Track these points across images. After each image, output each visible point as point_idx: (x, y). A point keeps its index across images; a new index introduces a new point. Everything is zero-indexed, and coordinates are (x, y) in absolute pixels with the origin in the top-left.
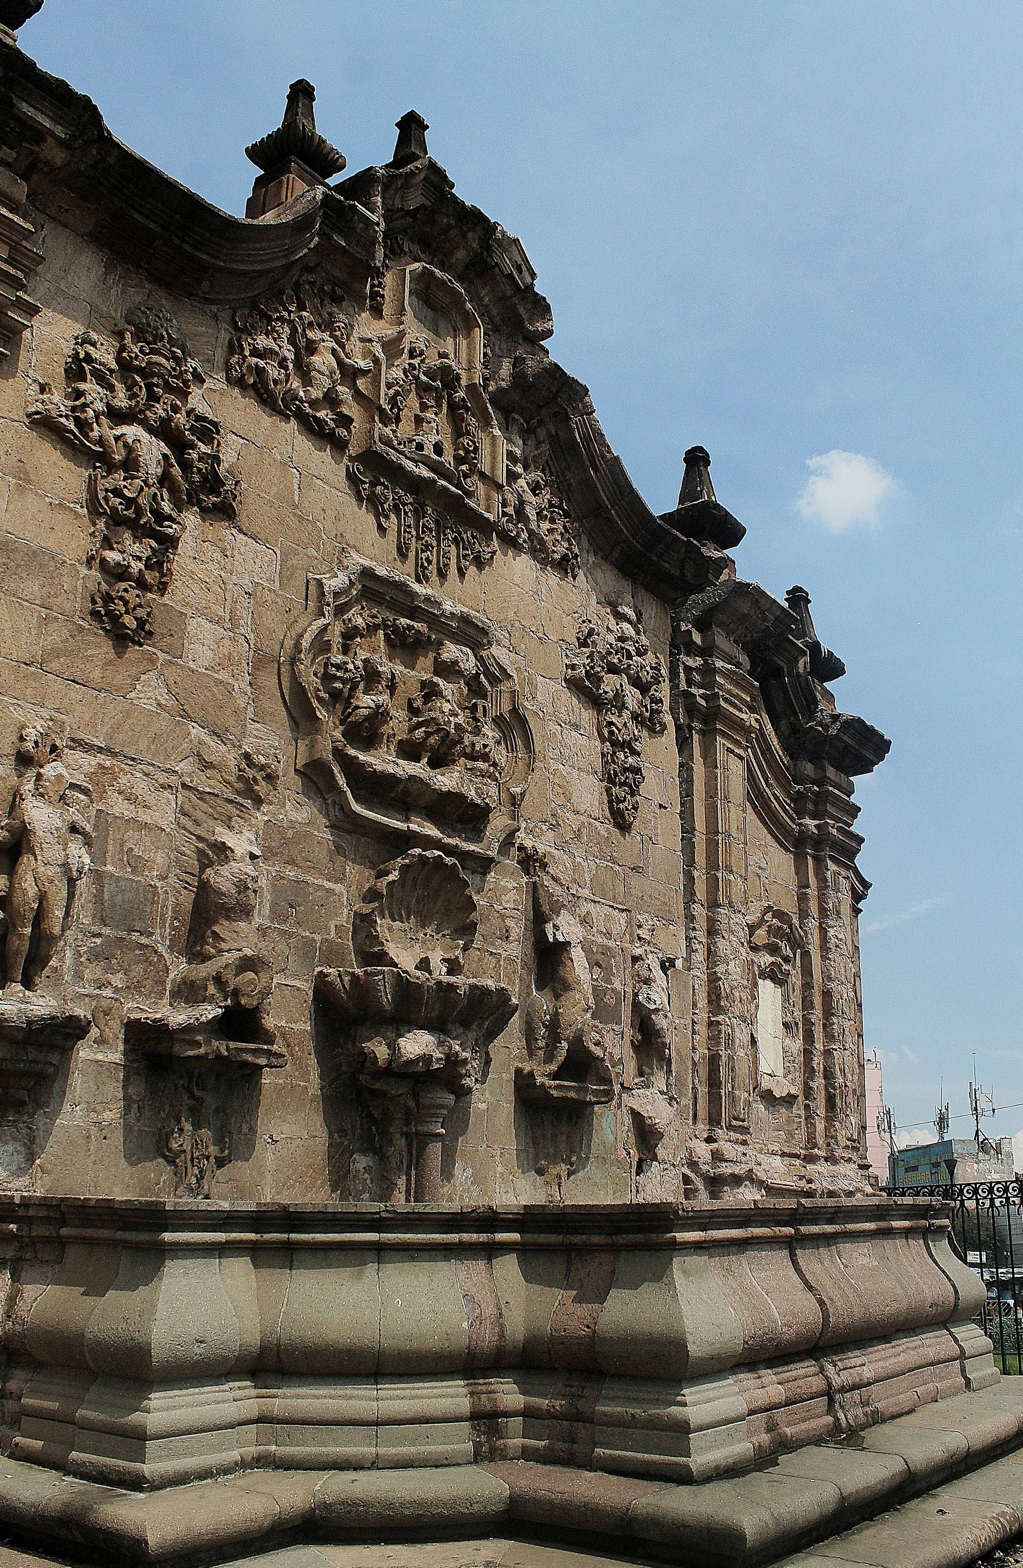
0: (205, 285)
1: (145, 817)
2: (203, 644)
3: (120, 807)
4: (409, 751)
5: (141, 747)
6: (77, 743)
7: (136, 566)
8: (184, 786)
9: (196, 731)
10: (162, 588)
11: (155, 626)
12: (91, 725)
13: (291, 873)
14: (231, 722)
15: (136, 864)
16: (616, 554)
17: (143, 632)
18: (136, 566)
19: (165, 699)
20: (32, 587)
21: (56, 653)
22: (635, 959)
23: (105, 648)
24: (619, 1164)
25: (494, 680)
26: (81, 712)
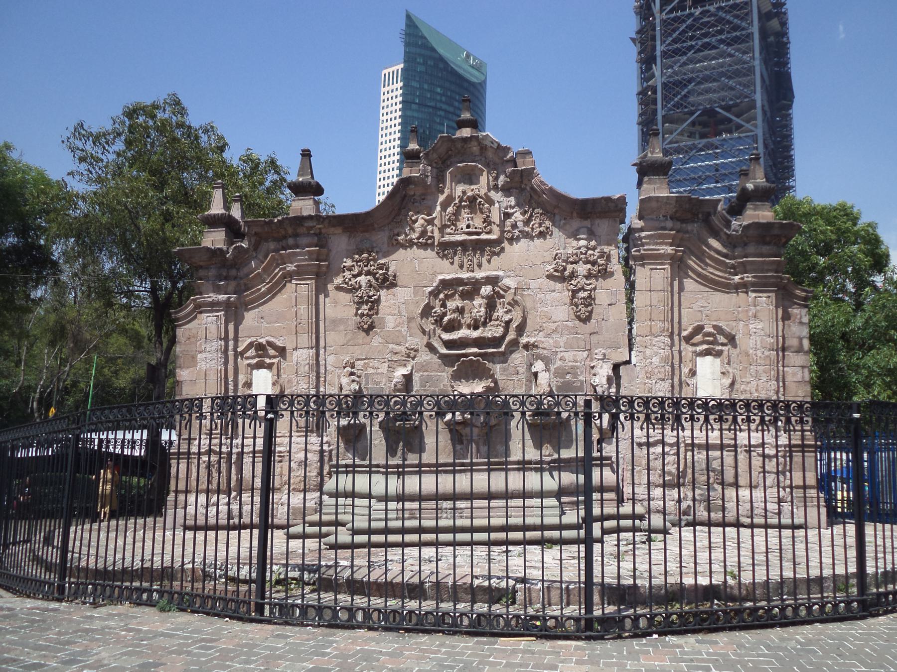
0: (376, 226)
1: (379, 371)
2: (390, 323)
3: (371, 371)
4: (469, 327)
5: (376, 355)
6: (358, 359)
7: (365, 312)
9: (391, 346)
10: (377, 313)
11: (376, 324)
12: (361, 354)
13: (426, 374)
14: (402, 339)
15: (377, 383)
16: (575, 214)
17: (371, 327)
18: (365, 312)
19: (380, 340)
20: (342, 328)
21: (349, 340)
22: (593, 367)
23: (364, 334)
25: (506, 291)
26: (358, 352)
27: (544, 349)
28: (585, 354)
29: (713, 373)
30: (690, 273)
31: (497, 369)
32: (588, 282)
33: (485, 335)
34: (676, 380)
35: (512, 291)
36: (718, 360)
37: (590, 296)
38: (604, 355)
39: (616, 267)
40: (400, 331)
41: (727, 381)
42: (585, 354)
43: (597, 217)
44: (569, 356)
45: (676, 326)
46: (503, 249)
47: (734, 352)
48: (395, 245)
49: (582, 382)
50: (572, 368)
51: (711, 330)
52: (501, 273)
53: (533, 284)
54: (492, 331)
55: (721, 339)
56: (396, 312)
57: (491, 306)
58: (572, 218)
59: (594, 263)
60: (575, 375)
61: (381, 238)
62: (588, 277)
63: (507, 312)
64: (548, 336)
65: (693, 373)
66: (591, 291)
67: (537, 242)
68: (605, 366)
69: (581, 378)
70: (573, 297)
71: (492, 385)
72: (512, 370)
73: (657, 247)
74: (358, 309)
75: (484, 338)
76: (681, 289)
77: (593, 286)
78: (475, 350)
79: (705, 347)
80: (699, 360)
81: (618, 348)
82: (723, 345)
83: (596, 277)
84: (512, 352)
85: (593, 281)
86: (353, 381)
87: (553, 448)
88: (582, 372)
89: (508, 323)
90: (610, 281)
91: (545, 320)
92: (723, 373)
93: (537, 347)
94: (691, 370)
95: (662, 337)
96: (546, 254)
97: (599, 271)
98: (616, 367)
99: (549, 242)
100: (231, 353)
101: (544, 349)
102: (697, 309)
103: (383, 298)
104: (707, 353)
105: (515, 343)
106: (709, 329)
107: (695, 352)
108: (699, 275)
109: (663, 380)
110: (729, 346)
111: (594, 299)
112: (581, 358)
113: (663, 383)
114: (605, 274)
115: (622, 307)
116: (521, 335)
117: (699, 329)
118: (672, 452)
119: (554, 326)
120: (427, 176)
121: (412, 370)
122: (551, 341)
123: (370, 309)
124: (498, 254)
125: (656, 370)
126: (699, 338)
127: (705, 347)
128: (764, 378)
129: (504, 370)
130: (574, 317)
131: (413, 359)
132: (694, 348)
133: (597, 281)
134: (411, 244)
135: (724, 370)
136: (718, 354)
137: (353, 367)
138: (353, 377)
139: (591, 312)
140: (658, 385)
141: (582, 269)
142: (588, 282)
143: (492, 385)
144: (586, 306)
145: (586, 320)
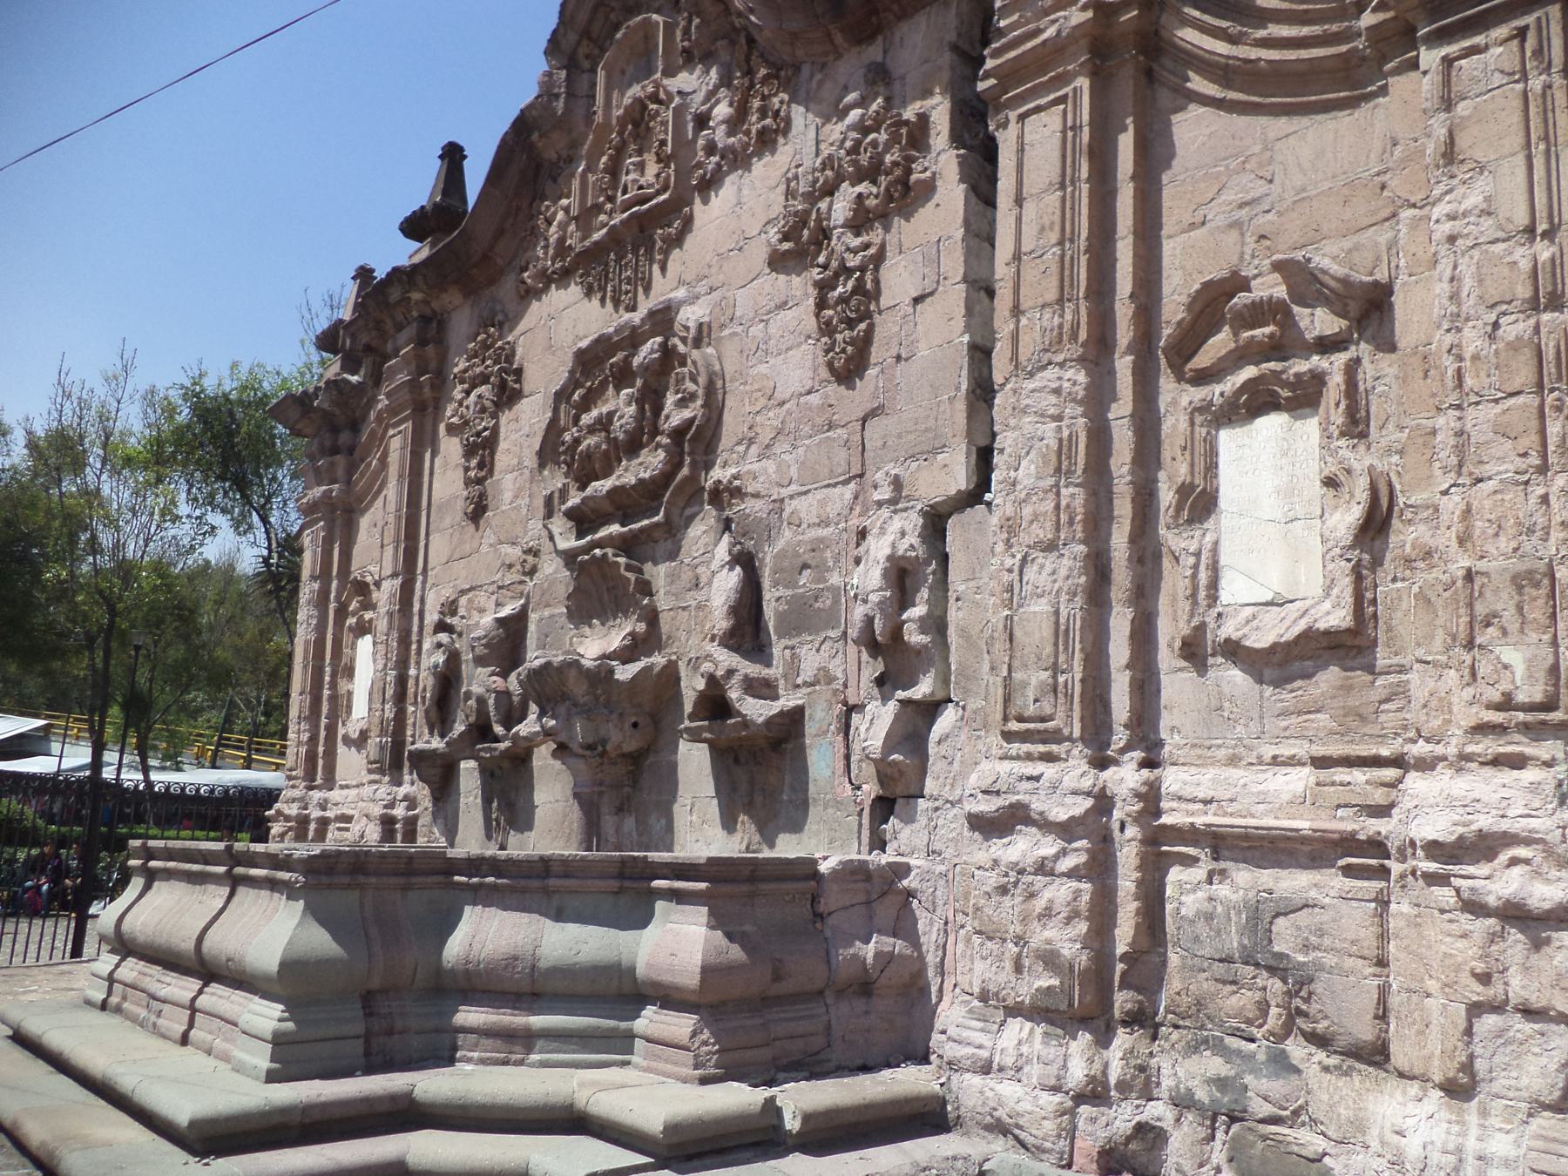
0: (499, 261)
6: (463, 592)
8: (500, 588)
14: (519, 530)
16: (839, 38)
24: (838, 804)
27: (756, 496)
28: (848, 491)
29: (1288, 492)
30: (1198, 83)
31: (658, 573)
32: (856, 242)
33: (624, 480)
34: (1119, 541)
35: (693, 332)
36: (1310, 427)
37: (859, 289)
38: (897, 483)
39: (943, 161)
40: (518, 508)
41: (1346, 518)
42: (848, 491)
43: (899, 19)
44: (805, 507)
45: (1124, 311)
46: (688, 222)
47: (1378, 369)
48: (529, 294)
49: (835, 590)
50: (816, 546)
51: (1281, 292)
52: (681, 293)
53: (743, 302)
54: (651, 462)
55: (1319, 321)
56: (515, 461)
57: (651, 400)
58: (839, 56)
59: (870, 173)
60: (822, 571)
61: (506, 289)
62: (861, 220)
63: (682, 403)
64: (766, 452)
65: (1200, 503)
66: (862, 269)
67: (758, 166)
68: (897, 523)
69: (835, 579)
70: (821, 304)
71: (641, 627)
72: (687, 575)
73: (1032, 26)
74: (467, 469)
75: (623, 487)
76: (1154, 155)
77: (872, 251)
78: (615, 528)
79: (1249, 372)
80: (1228, 439)
81: (935, 451)
82: (1326, 345)
83: (883, 217)
84: (690, 520)
85: (875, 236)
86: (439, 645)
87: (761, 830)
88: (837, 561)
89: (679, 434)
90: (925, 214)
91: (763, 402)
92: (1331, 482)
93: (737, 493)
94: (1184, 491)
95: (1051, 373)
96: (772, 196)
97: (889, 197)
98: (936, 523)
99: (784, 155)
100: (332, 606)
101: (756, 496)
102: (1221, 221)
103: (503, 430)
104: (1255, 403)
105: (692, 494)
106: (1270, 287)
107: (1204, 408)
108: (1223, 72)
109: (1050, 547)
110: (1364, 349)
111: (876, 294)
112: (838, 506)
113: (1049, 561)
114: (907, 195)
115: (954, 296)
116: (708, 466)
117: (1213, 304)
118: (1065, 864)
119: (773, 418)
120: (557, 96)
121: (524, 608)
122: (770, 466)
123: (481, 466)
124: (678, 241)
125: (1027, 511)
126: (1220, 343)
127: (1249, 372)
128: (1503, 462)
129: (673, 577)
130: (824, 373)
131: (532, 572)
132: (1196, 394)
133: (887, 229)
134: (549, 280)
135: (1332, 469)
136: (1303, 397)
137: (454, 613)
138: (443, 637)
139: (864, 345)
140: (1031, 573)
141: (840, 208)
142: (856, 242)
143: (641, 627)
144: (851, 324)
145: (848, 371)
